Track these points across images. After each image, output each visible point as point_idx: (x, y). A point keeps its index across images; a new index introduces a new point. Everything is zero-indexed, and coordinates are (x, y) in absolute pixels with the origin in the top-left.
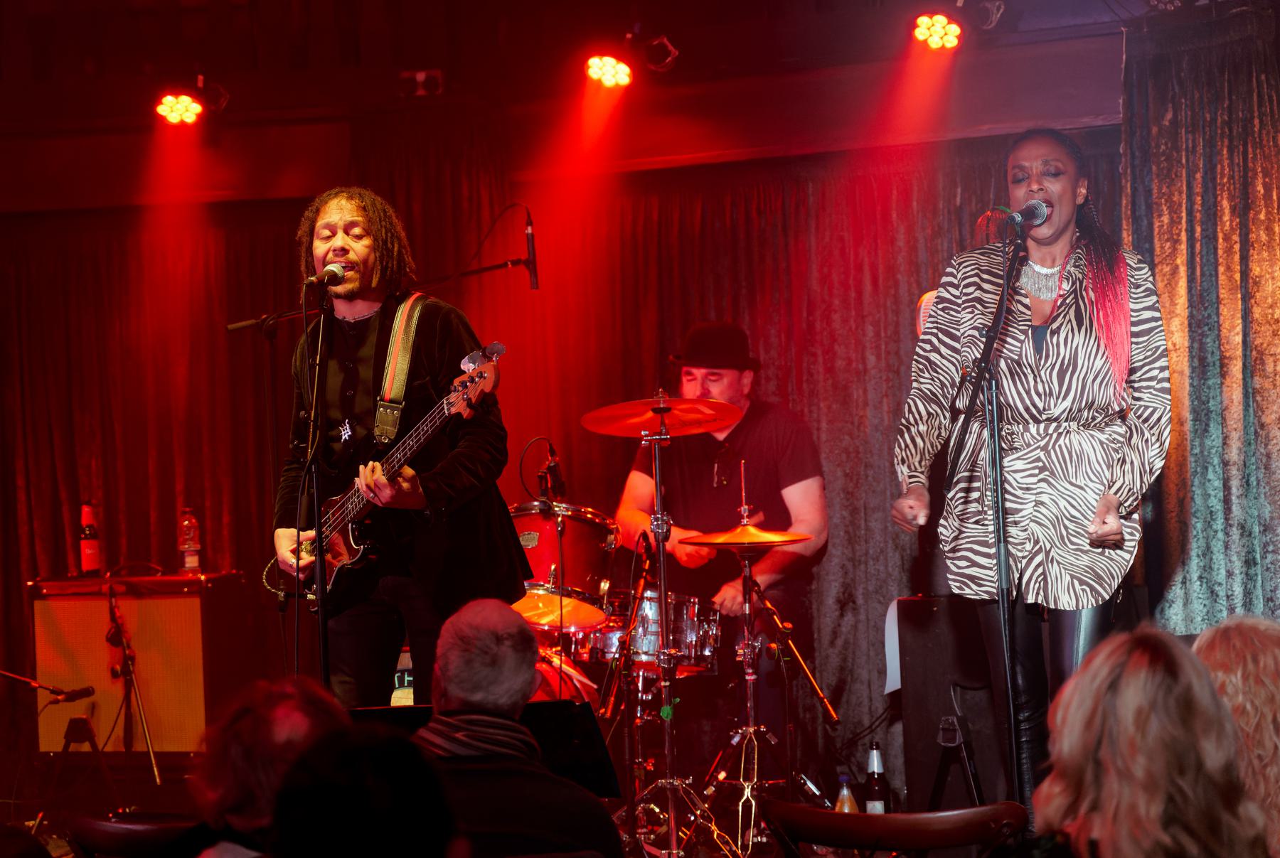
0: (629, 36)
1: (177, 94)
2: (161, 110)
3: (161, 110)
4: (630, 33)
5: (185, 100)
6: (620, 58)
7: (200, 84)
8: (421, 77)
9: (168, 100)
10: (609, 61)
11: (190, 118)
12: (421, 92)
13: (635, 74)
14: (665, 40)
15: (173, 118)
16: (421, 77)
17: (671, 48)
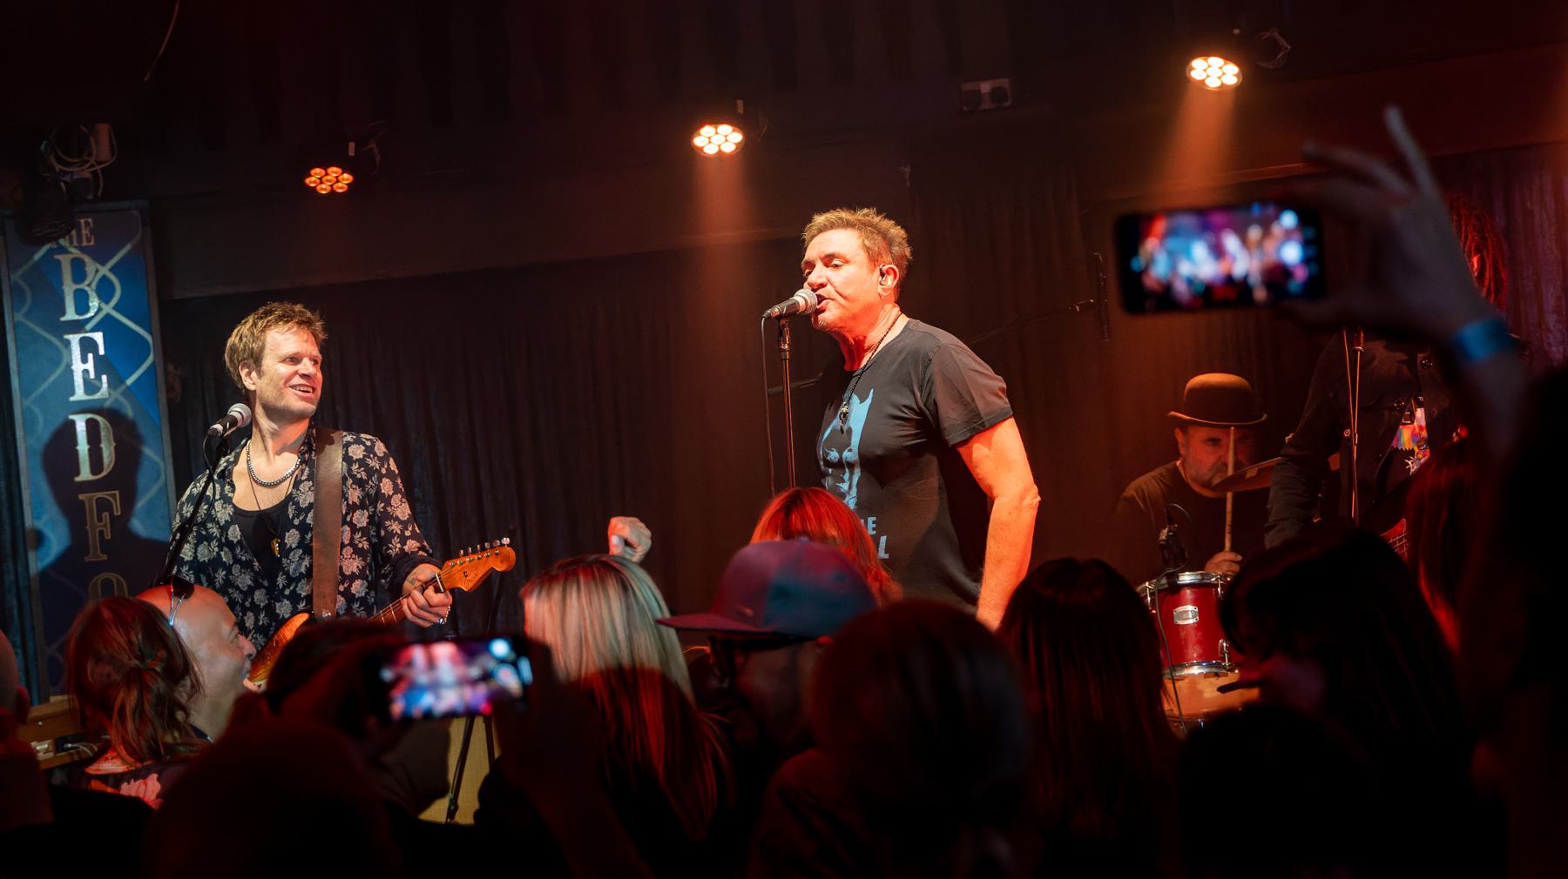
0: (1236, 31)
1: (715, 122)
2: (698, 141)
3: (698, 141)
4: (1237, 28)
5: (725, 129)
6: (1228, 58)
7: (740, 111)
8: (985, 87)
9: (707, 130)
10: (1215, 61)
11: (729, 148)
12: (986, 105)
13: (1245, 74)
14: (1276, 35)
15: (710, 150)
16: (985, 87)
17: (1283, 42)
